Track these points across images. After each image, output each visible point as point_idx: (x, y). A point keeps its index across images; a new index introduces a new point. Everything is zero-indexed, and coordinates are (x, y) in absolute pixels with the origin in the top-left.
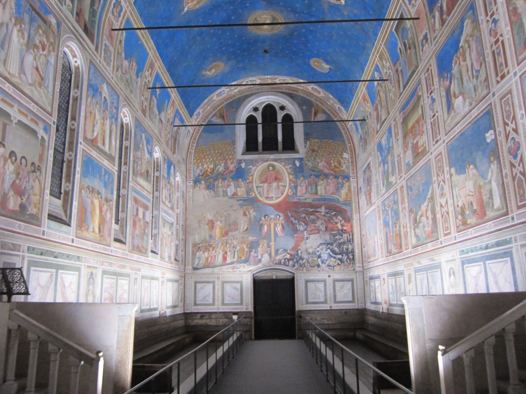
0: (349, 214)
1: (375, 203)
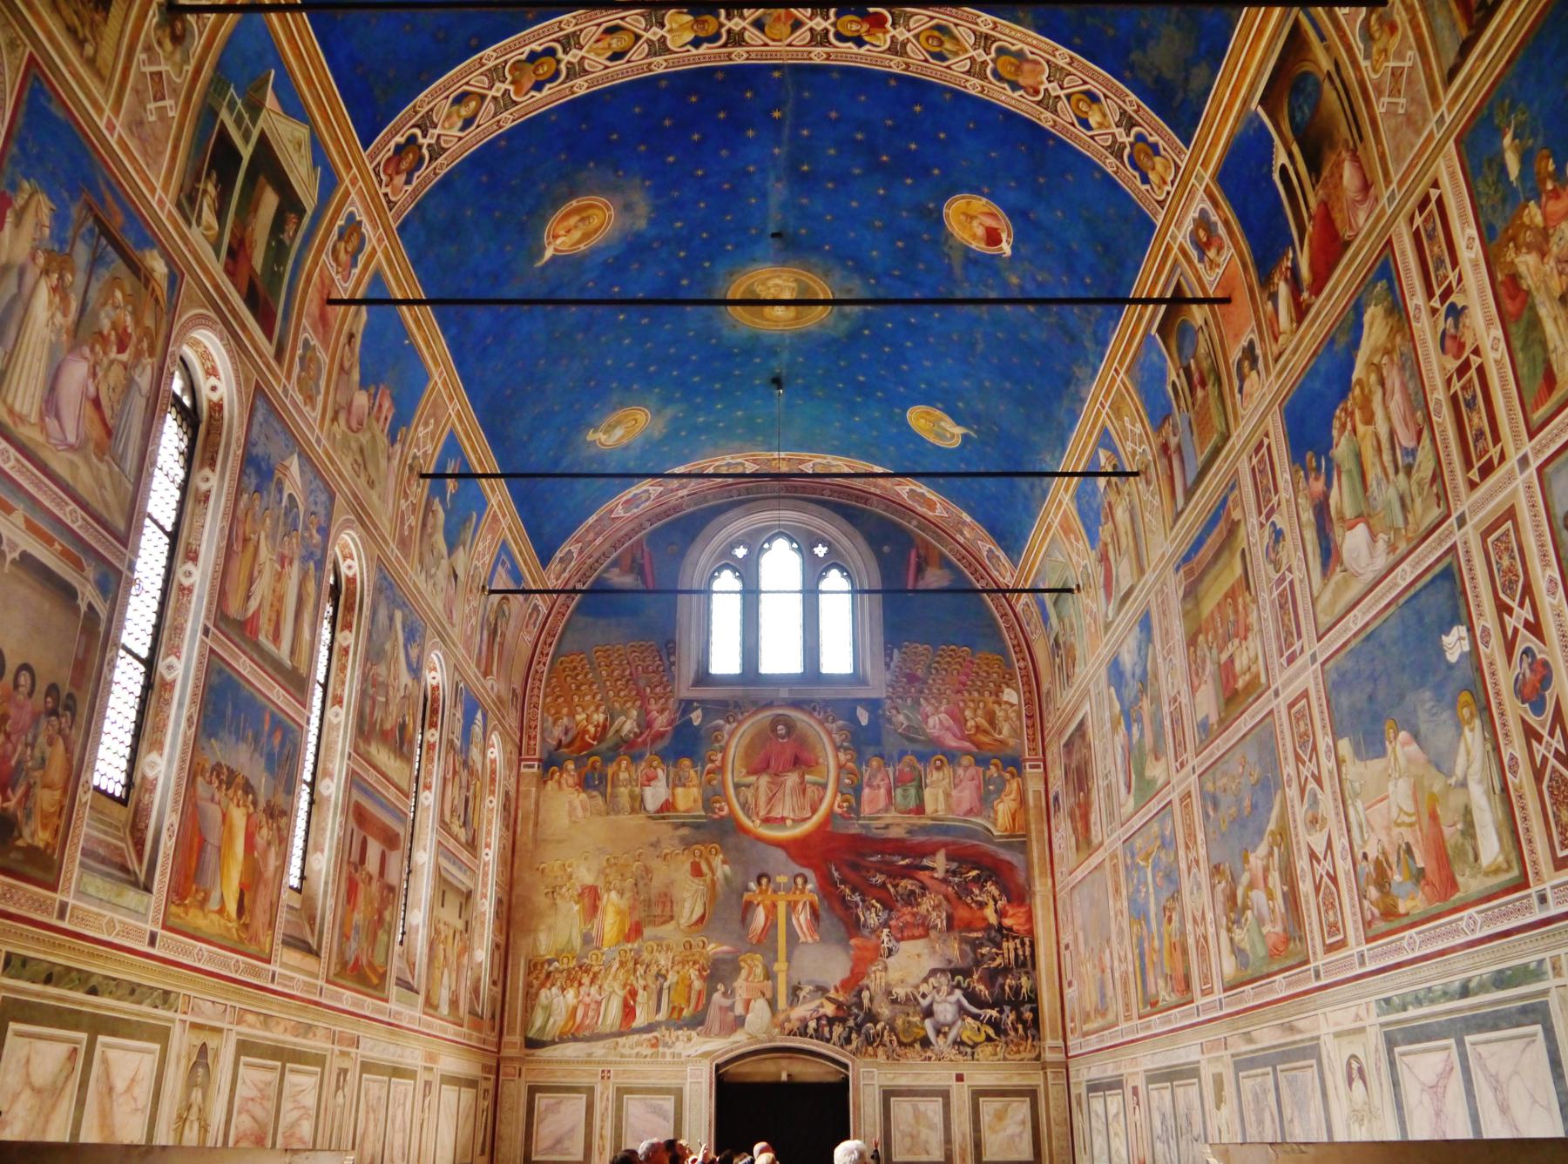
0: (1021, 878)
1: (1101, 844)
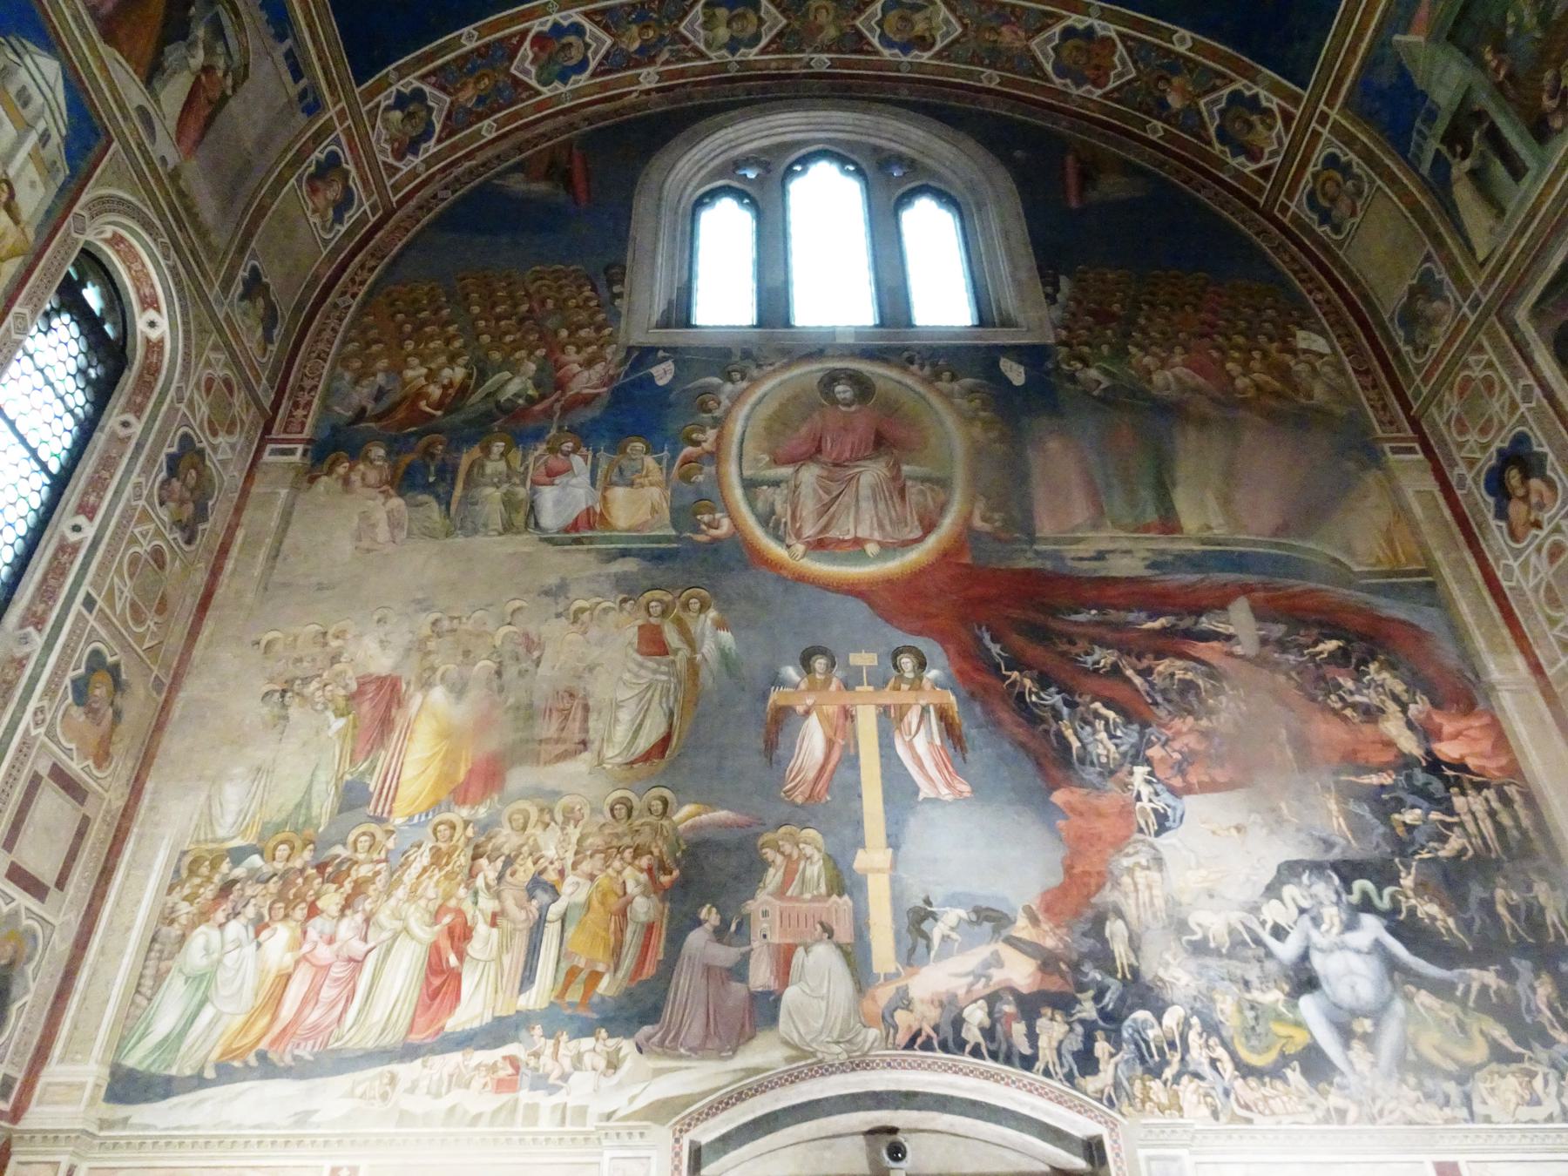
0: (1449, 655)
